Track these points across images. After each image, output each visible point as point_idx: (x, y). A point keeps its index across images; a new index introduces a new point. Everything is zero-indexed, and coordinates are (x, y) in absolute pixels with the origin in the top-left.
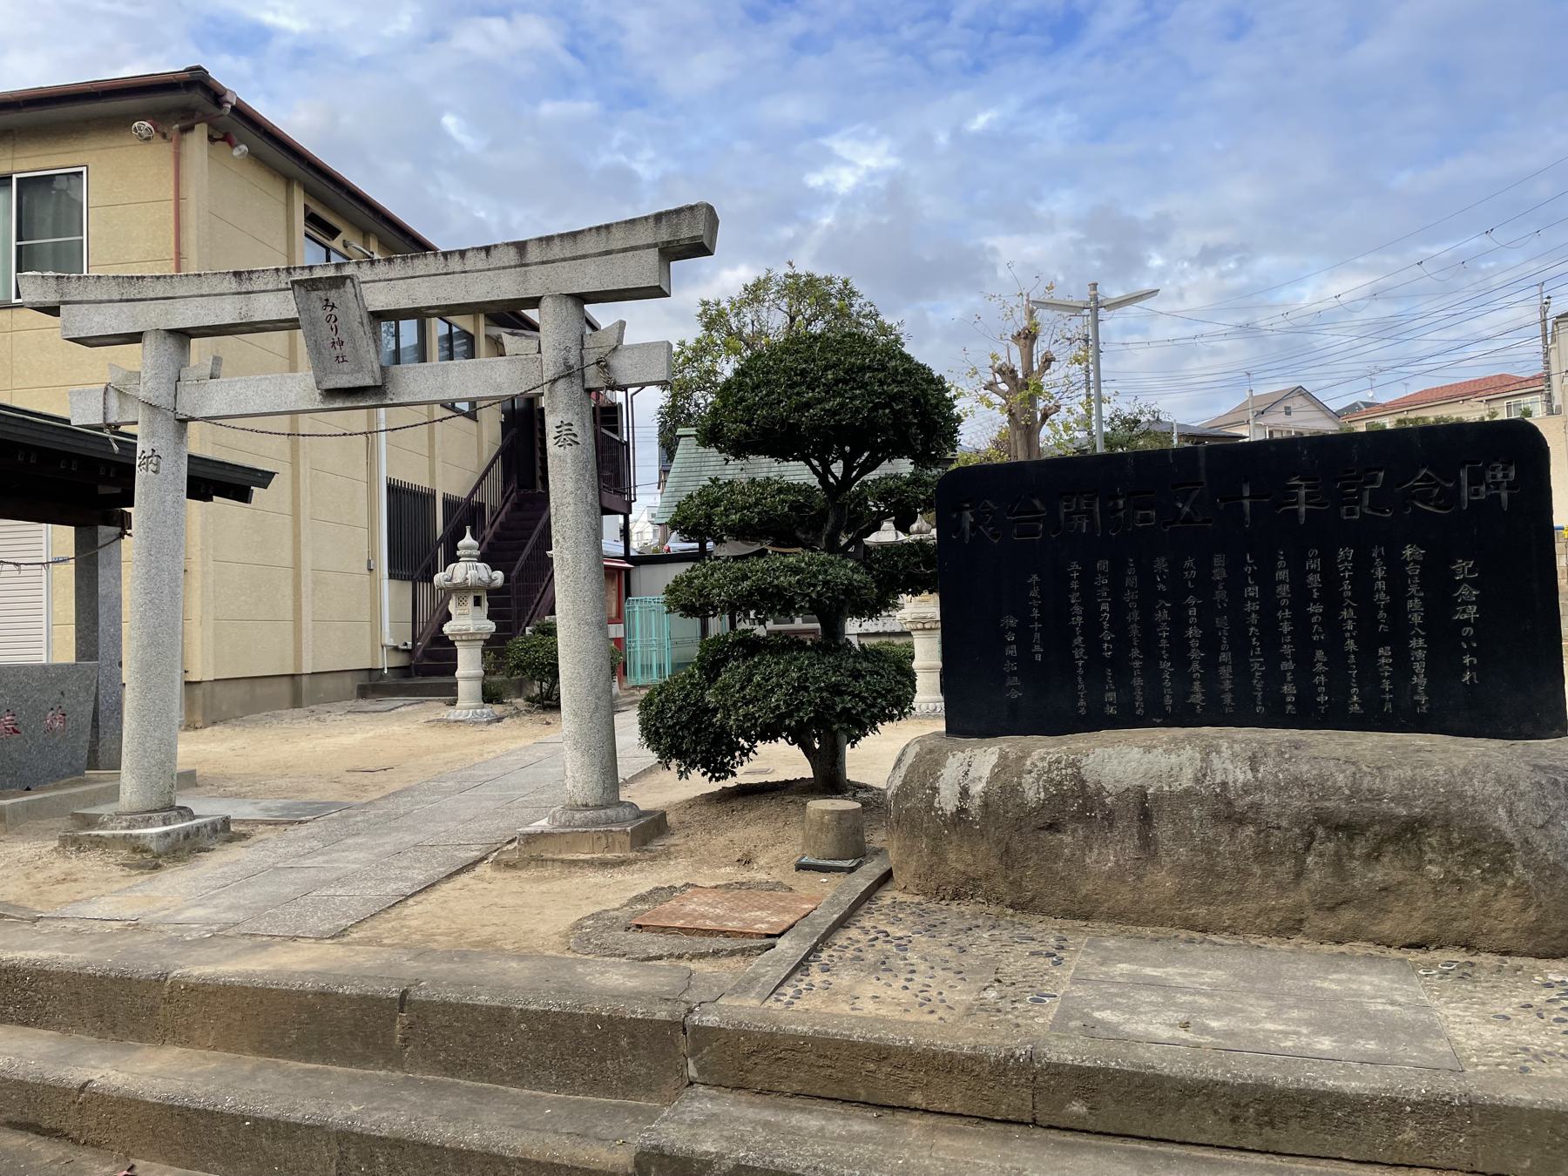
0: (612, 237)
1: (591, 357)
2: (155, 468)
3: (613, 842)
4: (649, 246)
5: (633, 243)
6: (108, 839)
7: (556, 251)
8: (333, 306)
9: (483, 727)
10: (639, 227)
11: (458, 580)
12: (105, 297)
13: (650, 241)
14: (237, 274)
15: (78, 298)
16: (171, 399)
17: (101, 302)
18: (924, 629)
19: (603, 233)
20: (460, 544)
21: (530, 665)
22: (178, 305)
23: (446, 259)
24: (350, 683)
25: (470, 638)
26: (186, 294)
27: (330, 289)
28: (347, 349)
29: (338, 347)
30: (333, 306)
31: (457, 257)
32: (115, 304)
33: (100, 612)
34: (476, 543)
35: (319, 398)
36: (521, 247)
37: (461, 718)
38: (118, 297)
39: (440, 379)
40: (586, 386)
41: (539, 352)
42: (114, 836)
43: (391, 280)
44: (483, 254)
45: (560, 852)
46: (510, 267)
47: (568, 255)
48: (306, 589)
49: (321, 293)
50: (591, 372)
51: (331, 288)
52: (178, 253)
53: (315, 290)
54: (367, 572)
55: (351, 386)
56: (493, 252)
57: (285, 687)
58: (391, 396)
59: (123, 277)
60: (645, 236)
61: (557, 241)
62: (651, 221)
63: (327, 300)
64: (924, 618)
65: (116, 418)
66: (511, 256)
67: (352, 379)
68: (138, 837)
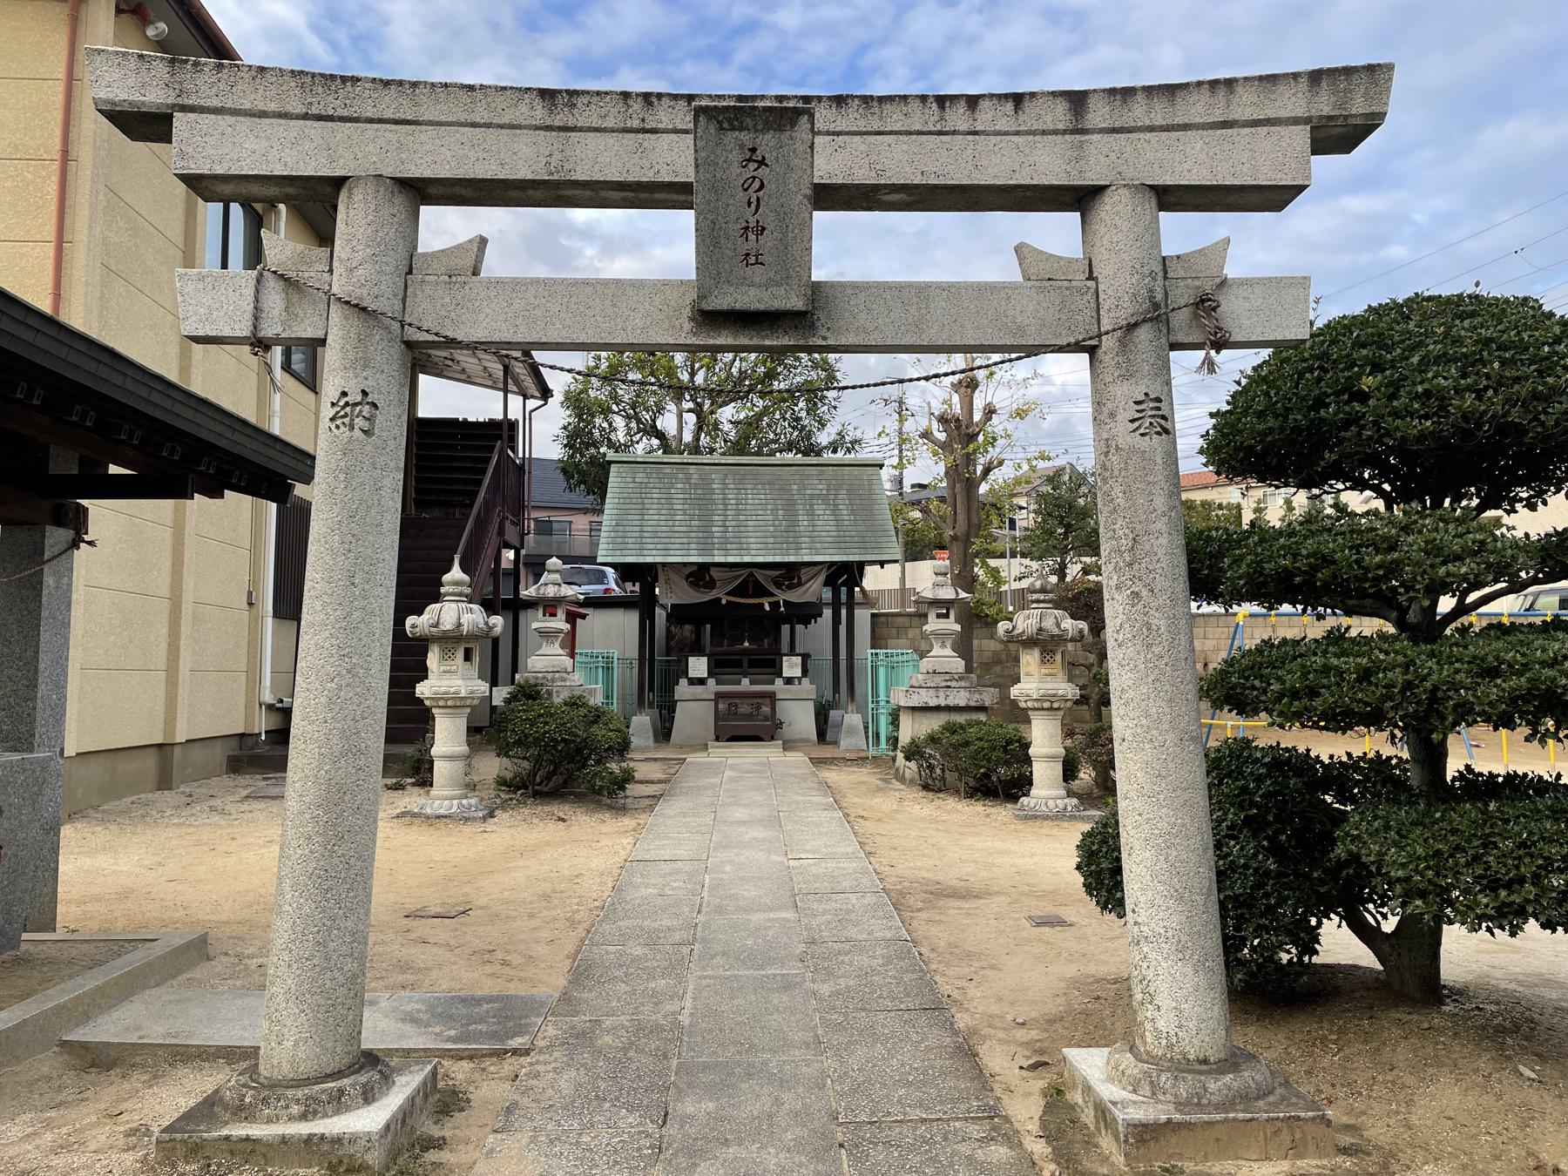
0: (1235, 99)
1: (1183, 295)
2: (366, 425)
3: (1304, 1138)
4: (1296, 121)
5: (1272, 114)
6: (269, 1145)
7: (1139, 112)
8: (762, 162)
9: (479, 827)
10: (1282, 88)
11: (448, 624)
12: (273, 107)
13: (1300, 112)
14: (547, 95)
15: (215, 102)
16: (398, 306)
17: (263, 114)
18: (1051, 709)
19: (1221, 92)
20: (446, 578)
21: (537, 741)
22: (423, 137)
23: (942, 107)
24: (219, 753)
25: (453, 704)
26: (443, 119)
27: (764, 131)
28: (768, 240)
29: (752, 237)
30: (762, 162)
31: (961, 108)
32: (292, 122)
33: (42, 666)
34: (466, 578)
35: (687, 326)
36: (1077, 100)
37: (442, 812)
38: (301, 109)
39: (913, 310)
40: (1172, 339)
41: (1091, 277)
42: (284, 1140)
43: (838, 134)
44: (1010, 106)
45: (1206, 1158)
46: (1056, 132)
47: (1159, 121)
48: (185, 629)
49: (745, 137)
50: (1181, 318)
51: (768, 126)
52: (65, 152)
53: (733, 129)
54: (245, 606)
55: (762, 307)
56: (1027, 104)
57: (150, 762)
58: (824, 332)
59: (313, 75)
60: (1292, 103)
61: (1140, 97)
62: (1303, 80)
63: (753, 150)
64: (1054, 695)
65: (279, 330)
66: (1059, 114)
67: (766, 295)
68: (338, 1140)
